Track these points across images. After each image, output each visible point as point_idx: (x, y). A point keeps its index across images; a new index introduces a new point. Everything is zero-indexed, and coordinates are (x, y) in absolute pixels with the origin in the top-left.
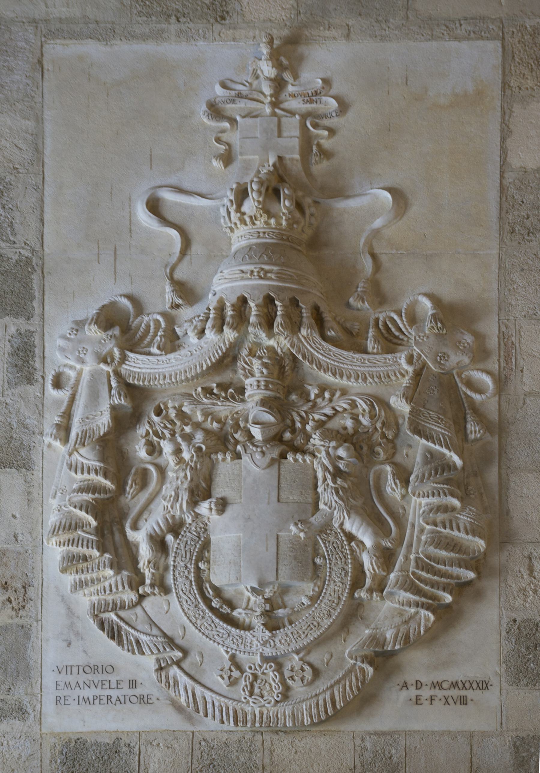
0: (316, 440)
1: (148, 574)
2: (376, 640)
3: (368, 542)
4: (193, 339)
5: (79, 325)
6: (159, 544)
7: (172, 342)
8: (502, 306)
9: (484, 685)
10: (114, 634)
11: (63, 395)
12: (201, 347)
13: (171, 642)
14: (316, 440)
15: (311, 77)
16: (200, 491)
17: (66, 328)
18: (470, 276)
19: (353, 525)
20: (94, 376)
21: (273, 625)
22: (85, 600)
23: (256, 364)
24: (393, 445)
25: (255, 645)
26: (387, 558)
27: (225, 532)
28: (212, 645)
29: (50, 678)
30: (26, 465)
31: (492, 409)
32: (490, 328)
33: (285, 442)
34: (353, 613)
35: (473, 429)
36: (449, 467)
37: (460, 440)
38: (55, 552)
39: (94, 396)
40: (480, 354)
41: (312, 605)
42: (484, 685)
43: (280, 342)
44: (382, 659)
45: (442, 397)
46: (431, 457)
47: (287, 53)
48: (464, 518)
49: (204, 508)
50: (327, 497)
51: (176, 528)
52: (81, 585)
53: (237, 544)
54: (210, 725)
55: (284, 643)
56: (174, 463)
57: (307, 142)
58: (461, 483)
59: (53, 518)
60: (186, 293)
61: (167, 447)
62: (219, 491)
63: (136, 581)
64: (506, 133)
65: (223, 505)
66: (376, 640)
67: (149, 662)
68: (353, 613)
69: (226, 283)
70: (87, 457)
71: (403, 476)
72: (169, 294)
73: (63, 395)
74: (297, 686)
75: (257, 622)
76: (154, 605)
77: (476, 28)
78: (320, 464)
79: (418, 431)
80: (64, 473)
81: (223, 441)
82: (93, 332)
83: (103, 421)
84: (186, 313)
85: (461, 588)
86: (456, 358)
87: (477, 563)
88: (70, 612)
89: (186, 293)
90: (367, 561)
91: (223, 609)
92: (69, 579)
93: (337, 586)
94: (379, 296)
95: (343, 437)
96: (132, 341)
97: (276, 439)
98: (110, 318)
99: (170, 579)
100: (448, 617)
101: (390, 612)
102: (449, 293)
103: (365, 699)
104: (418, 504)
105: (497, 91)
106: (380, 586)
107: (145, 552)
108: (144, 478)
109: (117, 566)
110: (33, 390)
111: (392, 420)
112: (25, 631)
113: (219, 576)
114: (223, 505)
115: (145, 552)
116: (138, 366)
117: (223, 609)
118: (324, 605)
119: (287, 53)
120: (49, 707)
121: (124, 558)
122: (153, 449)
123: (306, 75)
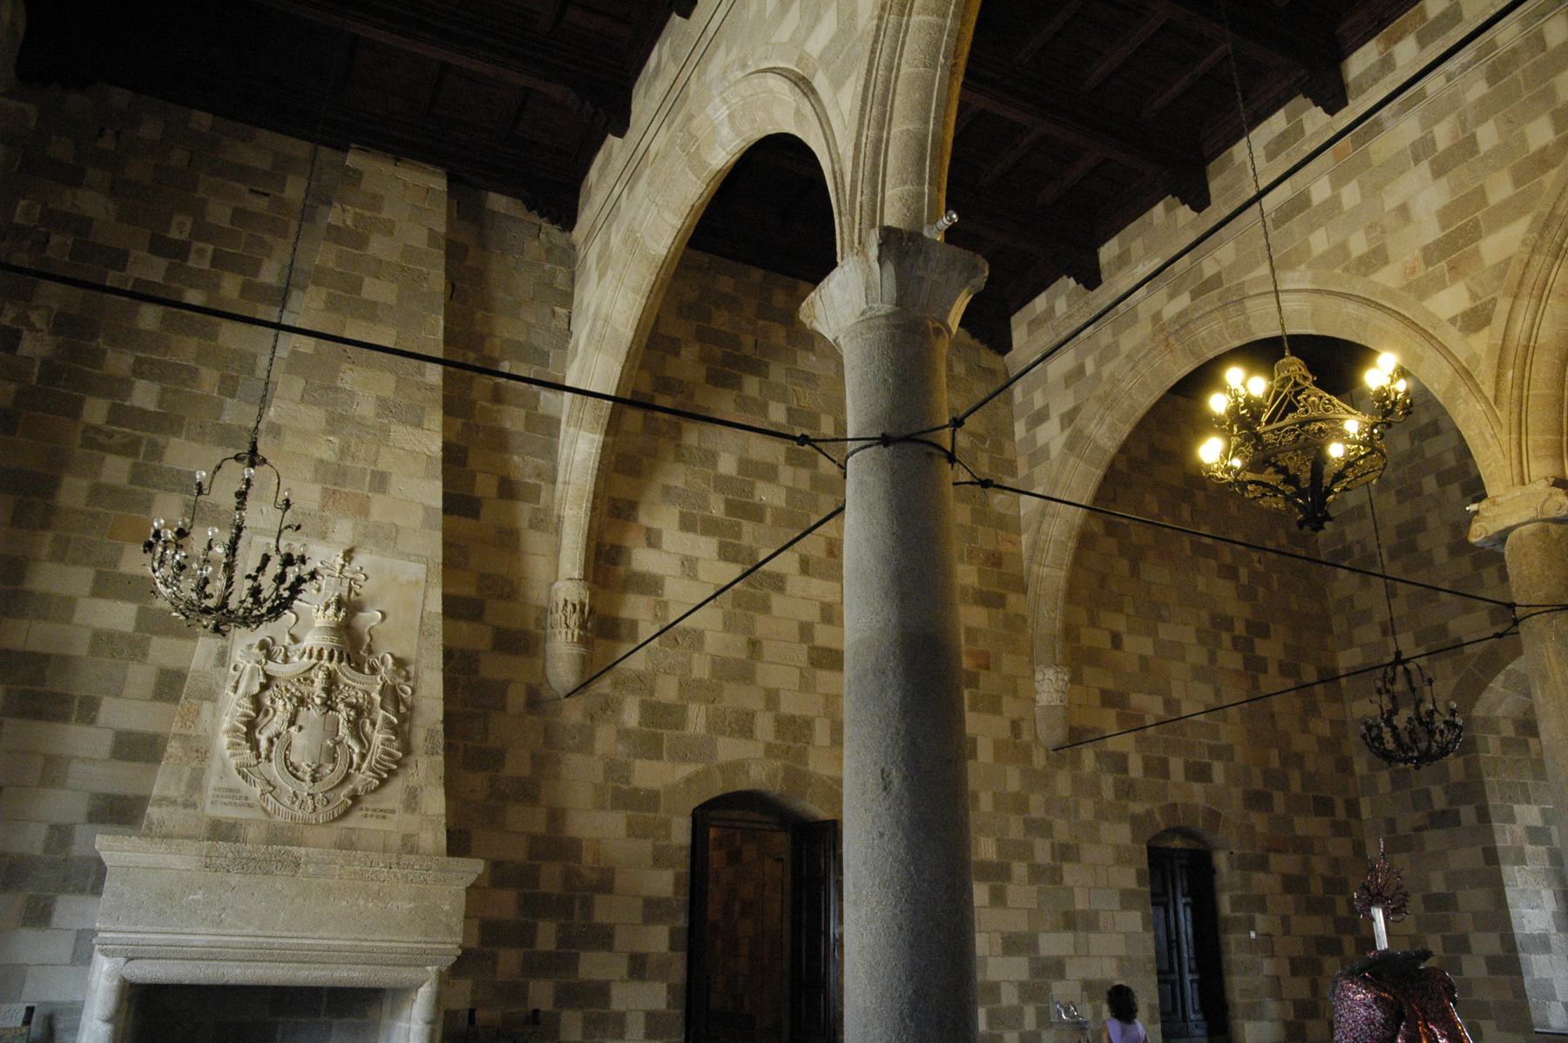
0: (341, 706)
1: (263, 754)
2: (355, 790)
3: (357, 750)
4: (296, 659)
5: (250, 646)
6: (271, 742)
7: (286, 660)
8: (417, 661)
9: (393, 812)
10: (245, 777)
11: (237, 674)
12: (299, 663)
13: (269, 783)
14: (341, 706)
15: (355, 565)
16: (292, 722)
17: (244, 647)
18: (407, 649)
19: (352, 743)
20: (253, 669)
21: (314, 780)
22: (233, 762)
23: (321, 675)
24: (370, 712)
25: (306, 788)
26: (363, 757)
27: (299, 739)
28: (287, 785)
29: (210, 792)
30: (215, 701)
31: (409, 701)
32: (411, 669)
33: (328, 705)
34: (347, 778)
35: (402, 709)
36: (391, 722)
37: (397, 713)
38: (224, 740)
39: (252, 677)
40: (408, 679)
41: (331, 774)
42: (393, 812)
43: (333, 665)
44: (355, 798)
45: (392, 695)
46: (386, 719)
47: (349, 555)
48: (396, 744)
49: (293, 729)
50: (344, 731)
51: (278, 735)
52: (233, 755)
53: (303, 745)
54: (278, 819)
55: (319, 788)
56: (282, 709)
57: (350, 589)
58: (395, 730)
59: (225, 725)
60: (295, 639)
61: (280, 703)
62: (300, 722)
63: (258, 756)
64: (425, 597)
65: (300, 728)
66: (355, 790)
67: (258, 791)
68: (347, 778)
69: (311, 640)
70: (246, 703)
71: (373, 724)
72: (287, 640)
73: (237, 674)
74: (319, 806)
75: (308, 778)
76: (264, 765)
77: (419, 558)
78: (342, 717)
79: (382, 707)
80: (234, 707)
81: (302, 701)
82: (255, 650)
83: (256, 689)
84: (293, 647)
85: (391, 772)
86: (399, 680)
87: (397, 762)
88: (224, 765)
89: (295, 639)
90: (356, 758)
91: (293, 771)
92: (228, 752)
93: (341, 767)
94: (370, 651)
95: (350, 705)
96: (269, 656)
97: (324, 704)
98: (263, 646)
99: (273, 756)
100: (383, 782)
101: (363, 778)
102: (398, 654)
103: (345, 814)
104: (378, 737)
105: (423, 582)
106: (359, 769)
107: (264, 744)
108: (267, 712)
109: (252, 749)
110: (224, 670)
111: (371, 701)
112: (203, 771)
113: (293, 758)
114: (300, 728)
115: (264, 744)
116: (272, 667)
117: (293, 771)
118: (336, 773)
119: (349, 555)
120: (208, 805)
121: (255, 746)
122: (273, 701)
123: (353, 564)
